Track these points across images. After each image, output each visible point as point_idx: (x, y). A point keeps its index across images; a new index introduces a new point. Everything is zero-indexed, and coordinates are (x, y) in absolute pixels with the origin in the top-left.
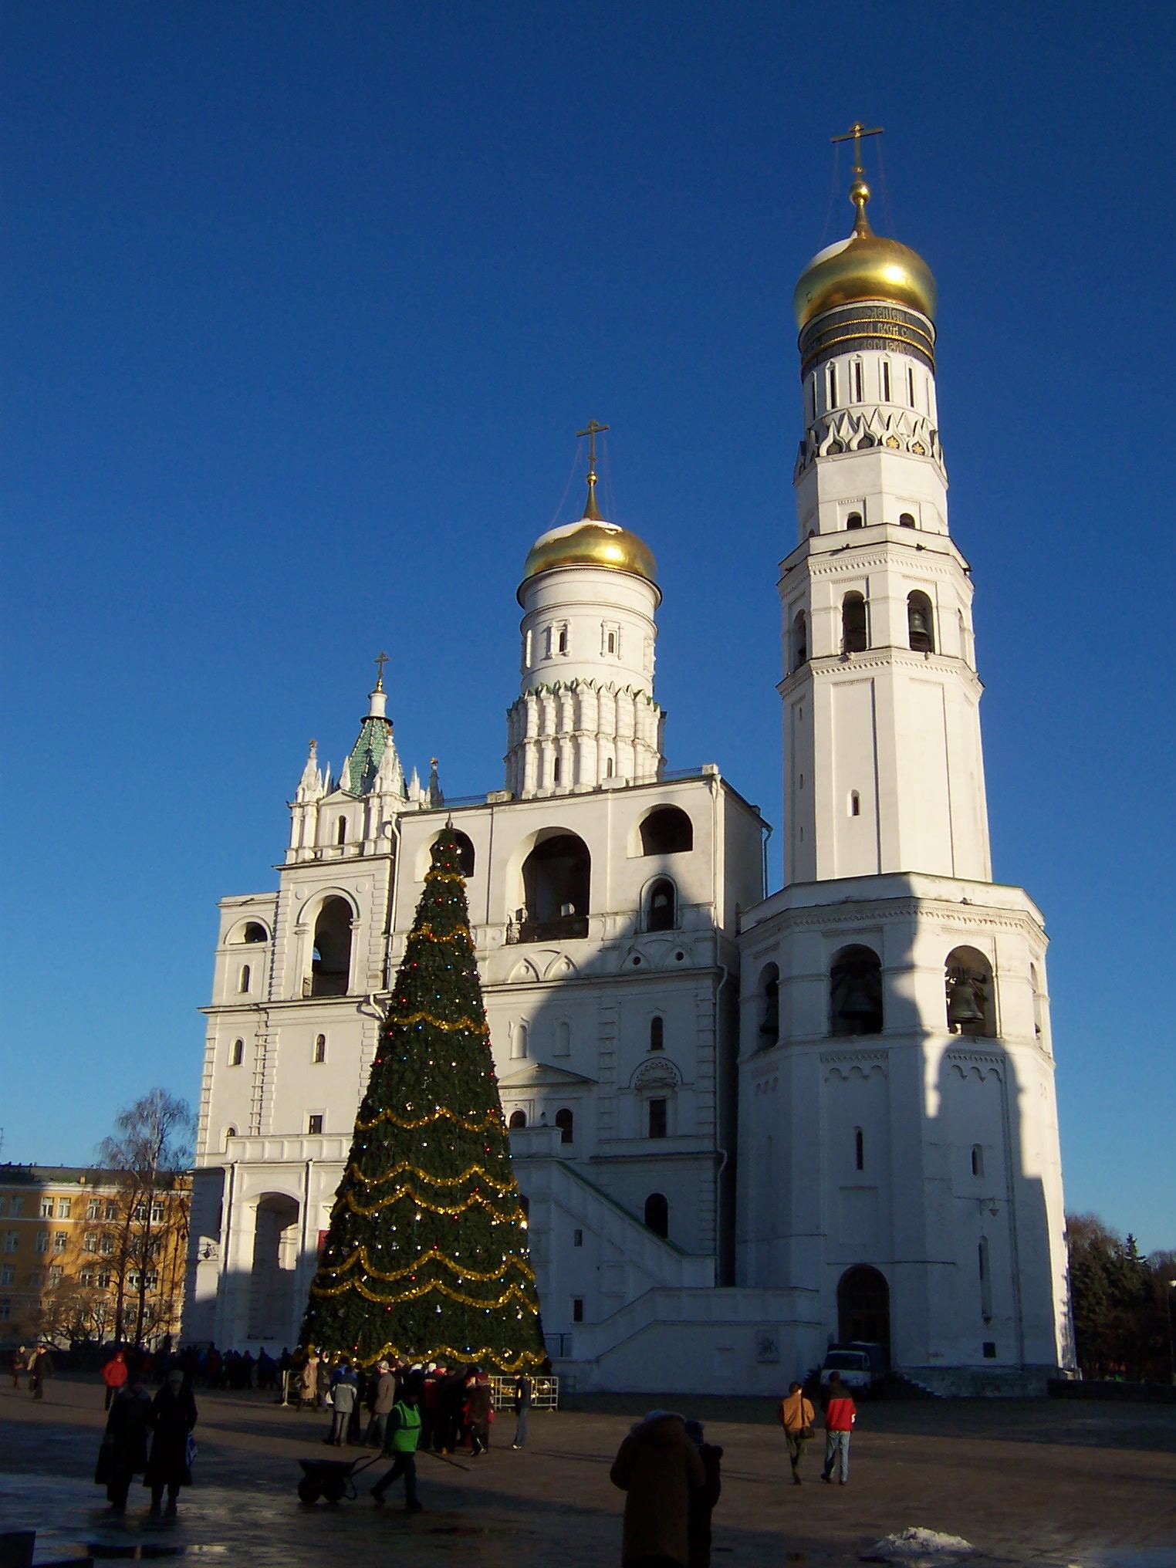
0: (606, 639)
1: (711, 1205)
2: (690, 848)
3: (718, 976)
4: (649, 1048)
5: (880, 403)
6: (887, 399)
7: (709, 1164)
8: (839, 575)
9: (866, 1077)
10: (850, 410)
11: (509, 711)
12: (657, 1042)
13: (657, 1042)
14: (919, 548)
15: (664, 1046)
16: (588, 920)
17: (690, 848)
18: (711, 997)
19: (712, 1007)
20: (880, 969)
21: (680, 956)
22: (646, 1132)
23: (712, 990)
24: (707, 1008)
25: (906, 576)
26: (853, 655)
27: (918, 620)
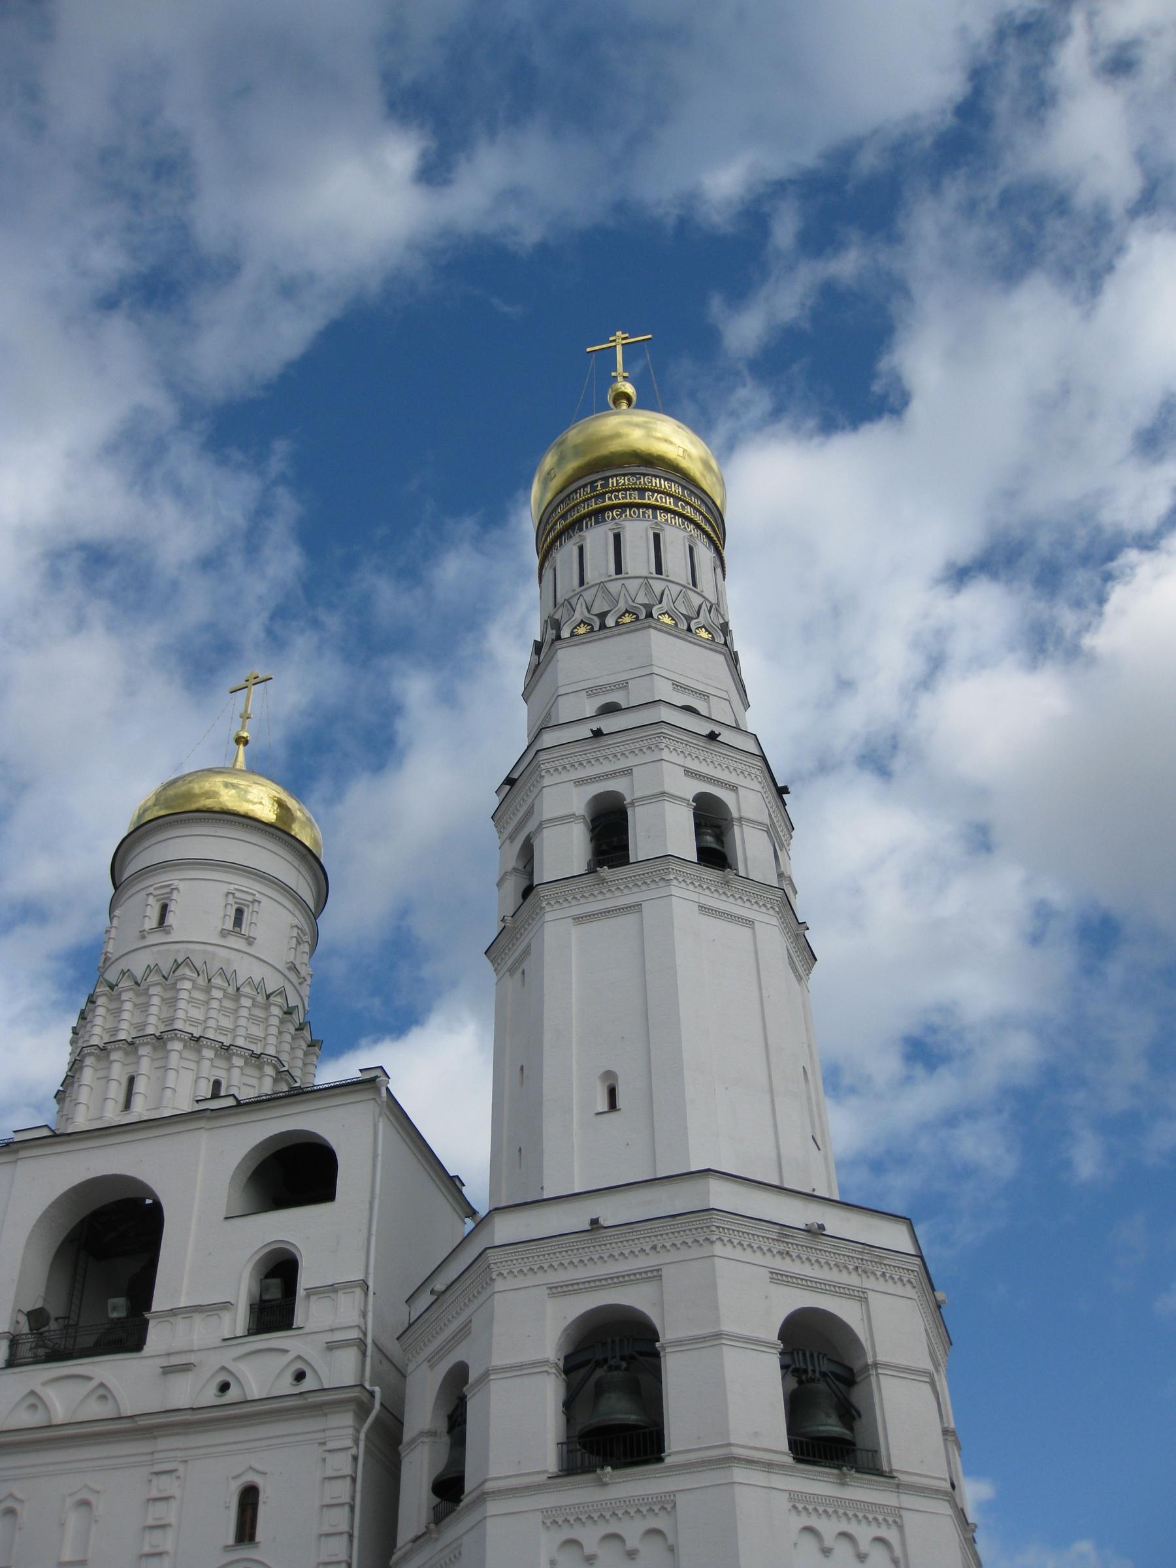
0: (232, 912)
3: (362, 1409)
4: (231, 1539)
5: (652, 575)
6: (659, 570)
10: (605, 584)
12: (246, 1531)
13: (246, 1531)
15: (258, 1538)
16: (146, 1322)
18: (349, 1443)
19: (350, 1458)
20: (657, 1344)
21: (300, 1376)
23: (351, 1431)
24: (342, 1464)
25: (689, 773)
26: (605, 871)
27: (711, 835)
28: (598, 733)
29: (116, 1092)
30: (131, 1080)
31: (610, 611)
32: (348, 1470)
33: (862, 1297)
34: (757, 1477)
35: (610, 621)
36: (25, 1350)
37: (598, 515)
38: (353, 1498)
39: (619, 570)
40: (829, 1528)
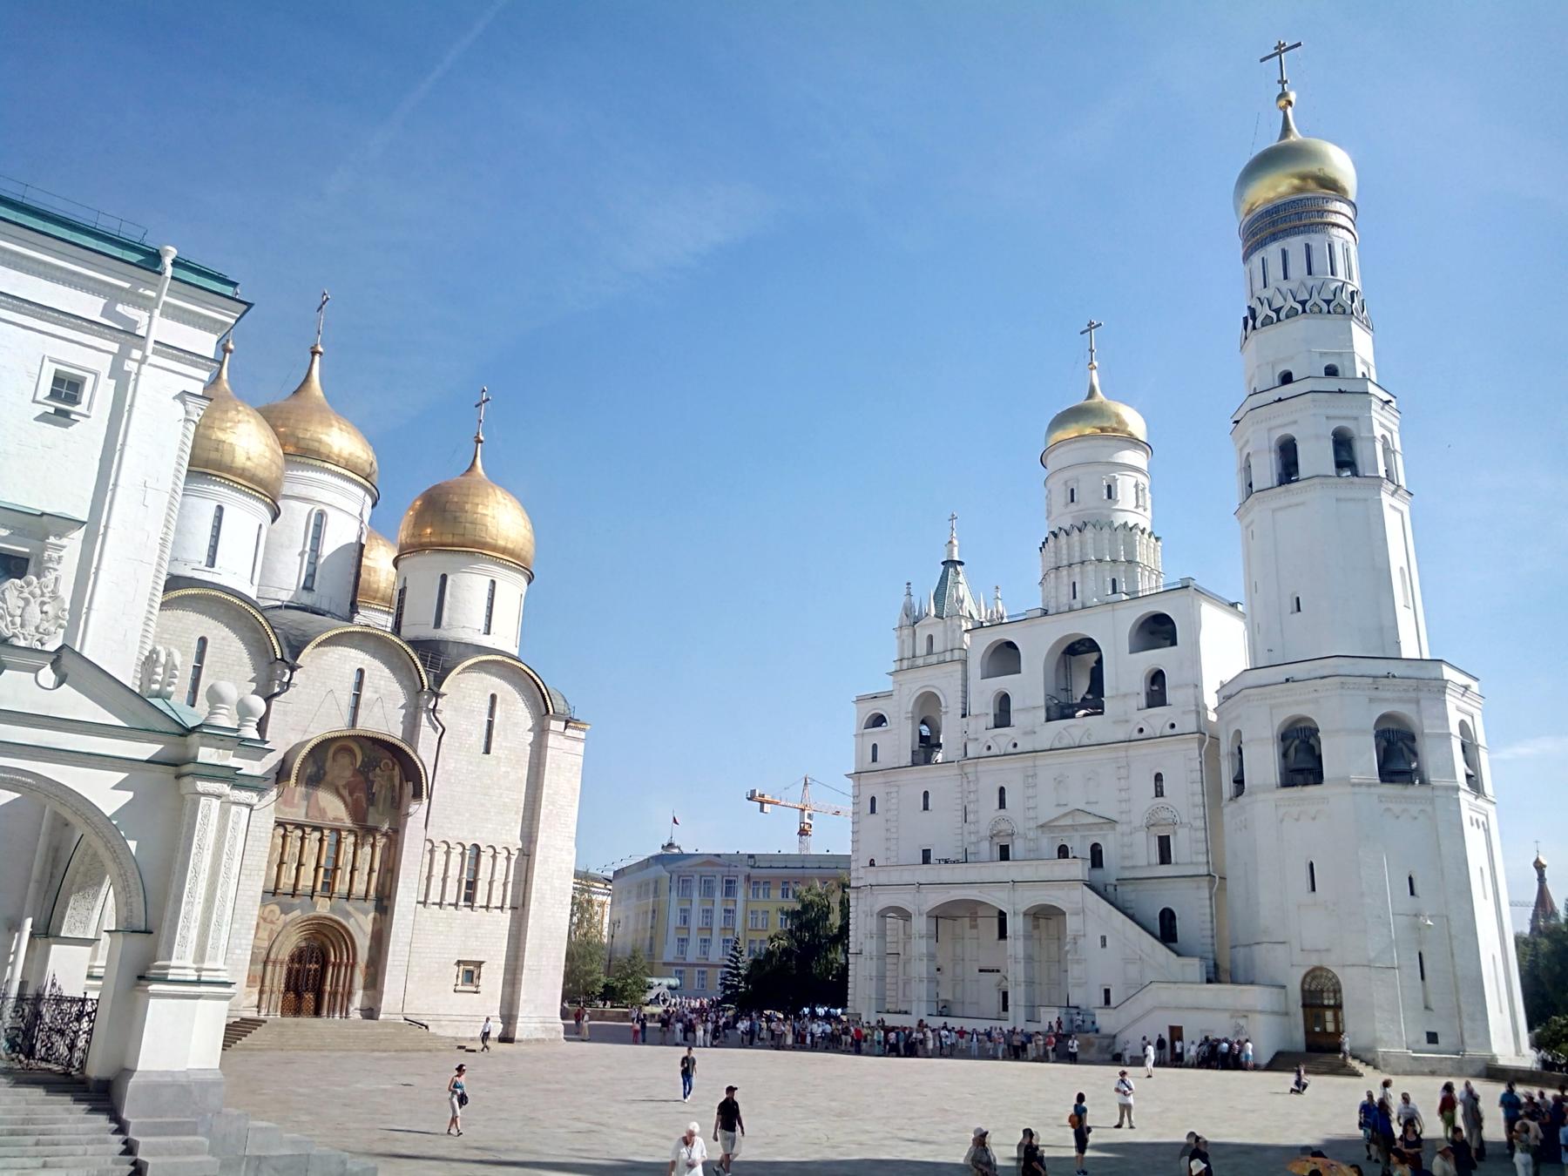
1: (1208, 918)
2: (1174, 643)
6: (1310, 273)
7: (1205, 883)
8: (1274, 423)
9: (1314, 819)
11: (1041, 549)
12: (1159, 793)
13: (1159, 793)
14: (1340, 391)
17: (1174, 643)
22: (1156, 858)
28: (1280, 400)
29: (1066, 590)
30: (1074, 584)
31: (1281, 308)
32: (1198, 767)
33: (1418, 702)
34: (1364, 789)
35: (1282, 315)
36: (1053, 714)
37: (1274, 237)
38: (1202, 778)
39: (1286, 277)
40: (1396, 808)
